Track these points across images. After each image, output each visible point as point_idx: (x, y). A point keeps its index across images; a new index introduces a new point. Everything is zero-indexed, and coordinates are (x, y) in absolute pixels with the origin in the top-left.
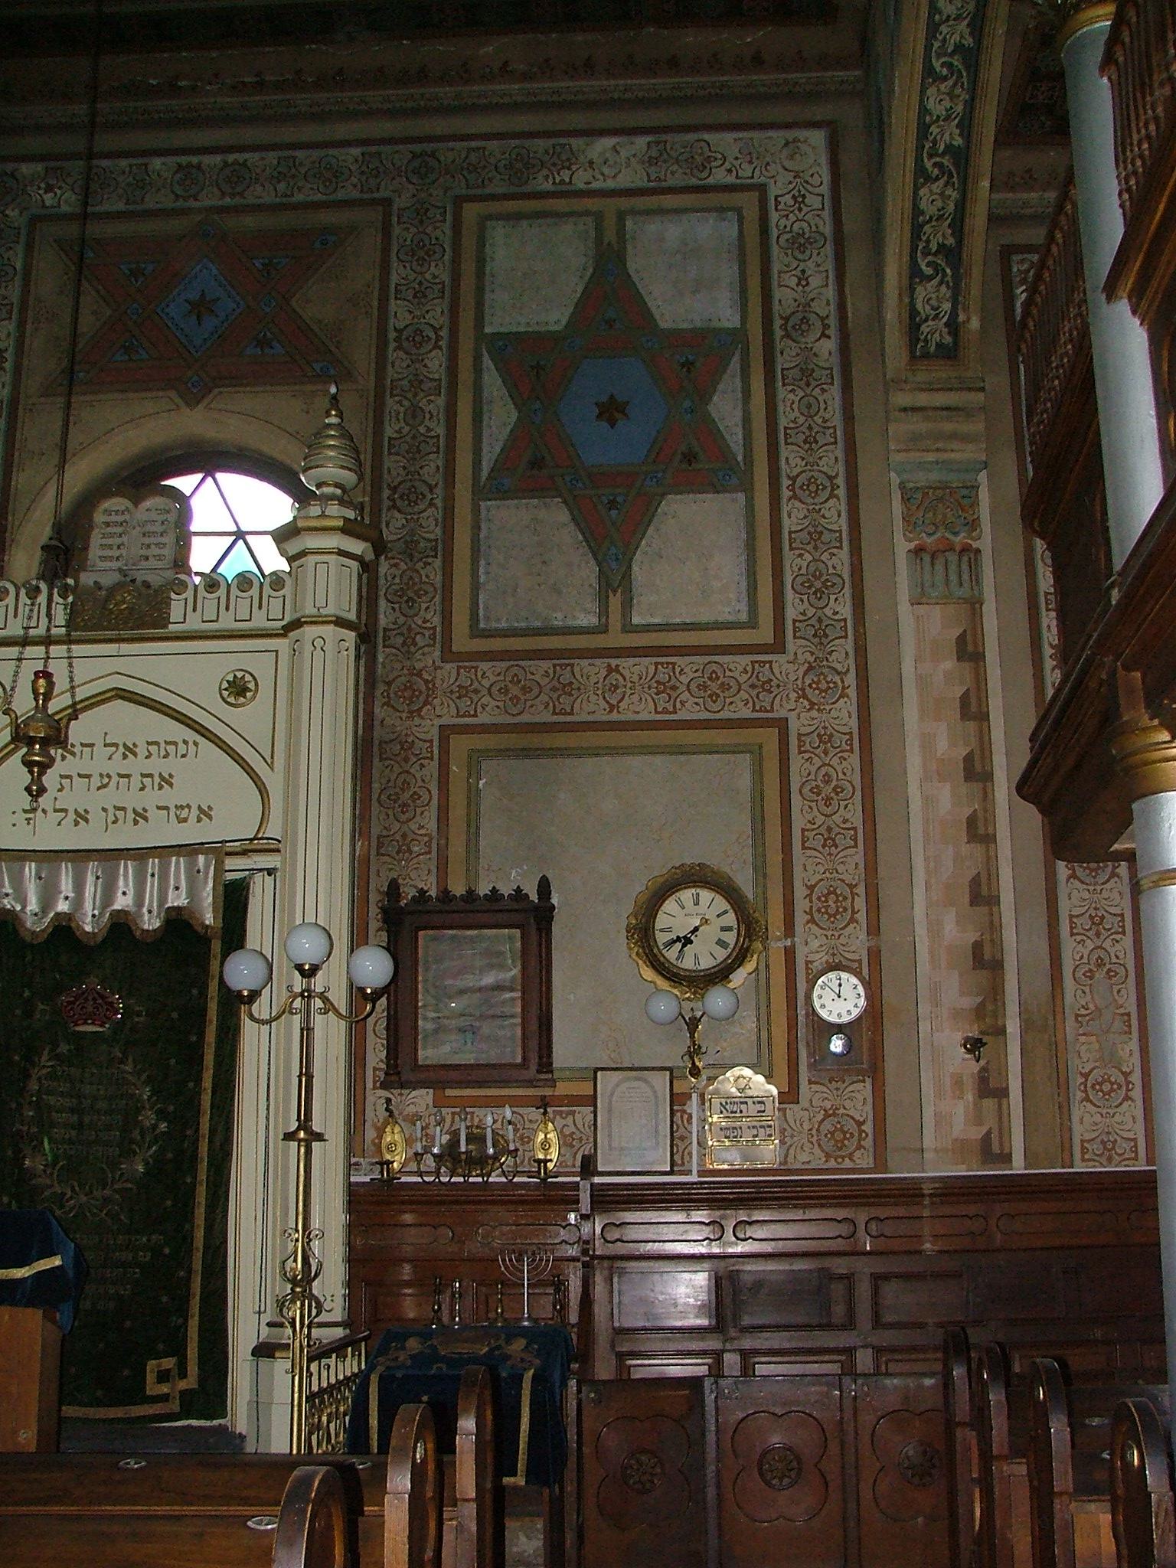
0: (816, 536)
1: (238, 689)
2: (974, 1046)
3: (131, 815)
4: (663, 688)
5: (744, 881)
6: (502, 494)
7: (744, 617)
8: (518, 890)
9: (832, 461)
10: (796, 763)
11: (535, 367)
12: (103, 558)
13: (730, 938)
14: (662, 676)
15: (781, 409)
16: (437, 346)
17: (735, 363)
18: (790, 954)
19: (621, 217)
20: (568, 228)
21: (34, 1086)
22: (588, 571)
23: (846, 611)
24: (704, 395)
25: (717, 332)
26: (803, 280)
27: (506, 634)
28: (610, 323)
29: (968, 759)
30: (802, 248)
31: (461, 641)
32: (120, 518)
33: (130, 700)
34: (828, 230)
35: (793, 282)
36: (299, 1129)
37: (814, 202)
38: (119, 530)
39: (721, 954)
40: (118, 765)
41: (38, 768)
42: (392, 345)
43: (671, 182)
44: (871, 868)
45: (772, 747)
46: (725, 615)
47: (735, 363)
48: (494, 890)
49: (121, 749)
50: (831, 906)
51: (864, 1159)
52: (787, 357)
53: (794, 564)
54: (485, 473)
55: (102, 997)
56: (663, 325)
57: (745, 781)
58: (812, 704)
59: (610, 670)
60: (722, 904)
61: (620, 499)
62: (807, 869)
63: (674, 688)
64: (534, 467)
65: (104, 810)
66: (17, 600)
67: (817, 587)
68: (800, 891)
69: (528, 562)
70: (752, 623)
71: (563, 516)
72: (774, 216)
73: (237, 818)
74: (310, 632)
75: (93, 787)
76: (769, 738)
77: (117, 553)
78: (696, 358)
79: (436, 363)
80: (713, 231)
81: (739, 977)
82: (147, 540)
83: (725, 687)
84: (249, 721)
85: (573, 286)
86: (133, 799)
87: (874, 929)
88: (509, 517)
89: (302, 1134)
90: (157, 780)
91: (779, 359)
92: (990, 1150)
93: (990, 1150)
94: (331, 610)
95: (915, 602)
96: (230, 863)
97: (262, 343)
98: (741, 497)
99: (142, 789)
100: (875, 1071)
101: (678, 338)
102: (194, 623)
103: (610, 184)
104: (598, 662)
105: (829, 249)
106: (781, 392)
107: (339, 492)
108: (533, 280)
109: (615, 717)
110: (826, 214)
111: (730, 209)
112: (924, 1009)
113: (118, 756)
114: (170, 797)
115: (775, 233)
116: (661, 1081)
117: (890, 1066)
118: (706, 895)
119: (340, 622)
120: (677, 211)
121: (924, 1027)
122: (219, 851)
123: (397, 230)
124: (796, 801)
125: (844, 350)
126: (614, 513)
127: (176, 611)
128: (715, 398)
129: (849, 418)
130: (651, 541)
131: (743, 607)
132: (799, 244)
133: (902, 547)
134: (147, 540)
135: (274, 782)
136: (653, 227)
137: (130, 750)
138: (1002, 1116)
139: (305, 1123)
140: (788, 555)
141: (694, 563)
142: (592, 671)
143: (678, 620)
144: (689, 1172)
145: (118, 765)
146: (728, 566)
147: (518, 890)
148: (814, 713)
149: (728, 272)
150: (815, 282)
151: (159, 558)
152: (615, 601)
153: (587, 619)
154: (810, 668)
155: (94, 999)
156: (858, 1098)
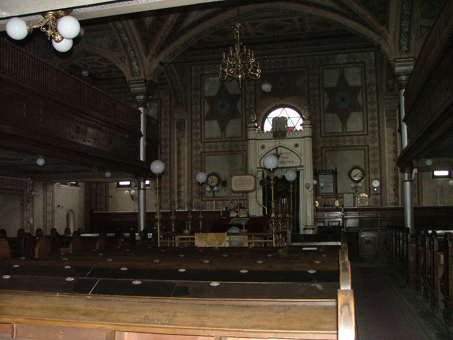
0: (373, 118)
1: (296, 145)
2: (394, 190)
5: (363, 167)
9: (375, 106)
10: (370, 151)
11: (331, 92)
13: (361, 176)
14: (351, 139)
18: (369, 177)
22: (341, 124)
23: (377, 129)
26: (371, 78)
29: (394, 150)
31: (323, 135)
34: (375, 69)
39: (360, 178)
44: (380, 166)
45: (367, 149)
50: (375, 171)
51: (379, 205)
52: (369, 90)
53: (370, 122)
57: (363, 153)
60: (360, 171)
62: (372, 166)
64: (332, 109)
67: (373, 125)
68: (371, 169)
69: (332, 123)
70: (364, 131)
73: (297, 163)
74: (306, 138)
76: (366, 148)
78: (355, 91)
81: (362, 181)
84: (298, 150)
87: (381, 174)
88: (329, 116)
92: (396, 204)
93: (396, 204)
95: (387, 127)
96: (298, 169)
100: (381, 194)
102: (290, 137)
103: (342, 62)
106: (368, 96)
108: (331, 79)
112: (387, 185)
114: (289, 160)
116: (352, 195)
117: (383, 192)
118: (358, 170)
119: (310, 137)
121: (388, 187)
122: (296, 167)
125: (377, 89)
127: (287, 135)
129: (377, 99)
133: (385, 119)
138: (398, 199)
141: (355, 123)
146: (360, 123)
149: (360, 76)
152: (344, 128)
156: (378, 197)
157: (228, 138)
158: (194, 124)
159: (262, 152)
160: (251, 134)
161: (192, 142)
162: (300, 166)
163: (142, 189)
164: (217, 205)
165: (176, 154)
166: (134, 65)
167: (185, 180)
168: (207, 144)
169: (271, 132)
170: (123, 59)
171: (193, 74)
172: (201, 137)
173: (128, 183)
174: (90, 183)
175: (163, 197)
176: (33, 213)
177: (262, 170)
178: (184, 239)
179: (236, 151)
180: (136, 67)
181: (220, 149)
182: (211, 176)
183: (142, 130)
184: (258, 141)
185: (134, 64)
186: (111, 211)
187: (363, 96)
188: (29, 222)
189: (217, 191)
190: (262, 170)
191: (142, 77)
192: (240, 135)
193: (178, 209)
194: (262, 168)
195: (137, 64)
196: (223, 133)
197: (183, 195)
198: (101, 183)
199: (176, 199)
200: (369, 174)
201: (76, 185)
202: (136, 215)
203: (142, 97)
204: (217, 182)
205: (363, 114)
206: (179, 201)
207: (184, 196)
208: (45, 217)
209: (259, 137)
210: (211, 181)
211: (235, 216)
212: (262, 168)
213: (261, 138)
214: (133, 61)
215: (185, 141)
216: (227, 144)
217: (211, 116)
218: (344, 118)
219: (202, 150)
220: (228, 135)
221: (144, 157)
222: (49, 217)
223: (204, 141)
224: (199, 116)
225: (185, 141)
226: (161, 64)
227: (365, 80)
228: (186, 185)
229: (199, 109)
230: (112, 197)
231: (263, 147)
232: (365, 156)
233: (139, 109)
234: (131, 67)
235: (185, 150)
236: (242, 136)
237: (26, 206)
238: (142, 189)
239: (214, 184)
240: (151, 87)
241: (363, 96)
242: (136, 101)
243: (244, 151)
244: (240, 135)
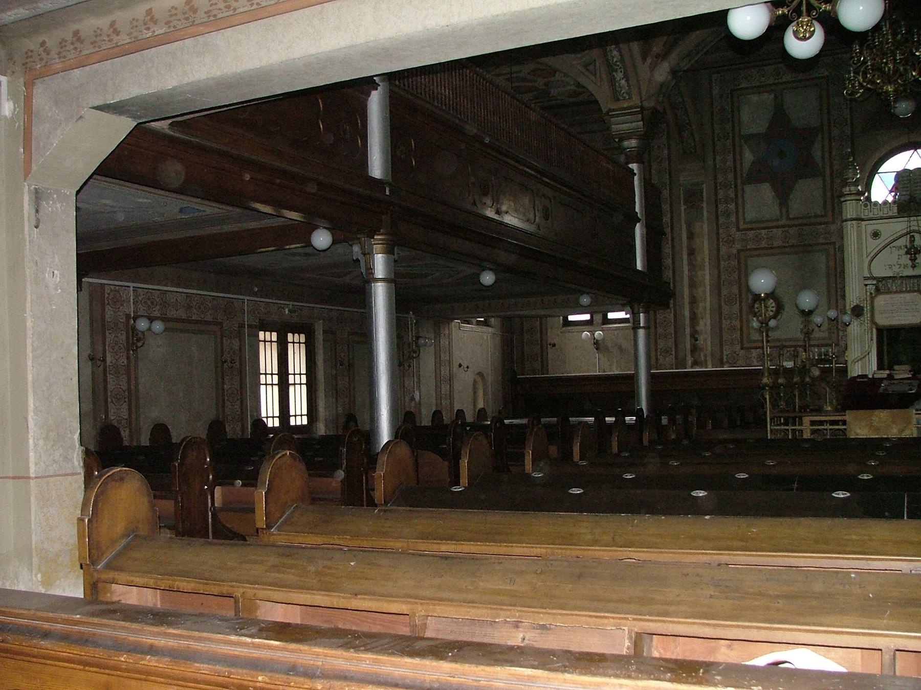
41: (913, 260)
158: (721, 193)
160: (850, 209)
161: (718, 229)
163: (643, 327)
165: (685, 257)
166: (618, 79)
167: (705, 308)
168: (751, 234)
169: (894, 202)
170: (591, 68)
171: (716, 91)
172: (737, 219)
173: (587, 317)
174: (509, 318)
175: (661, 344)
176: (419, 382)
177: (875, 282)
178: (821, 423)
179: (815, 246)
180: (623, 82)
181: (777, 243)
183: (637, 210)
184: (864, 223)
185: (619, 75)
186: (555, 372)
188: (413, 399)
189: (776, 328)
190: (875, 282)
191: (636, 101)
193: (692, 367)
194: (874, 278)
195: (626, 76)
196: (784, 210)
197: (701, 338)
198: (532, 317)
199: (688, 346)
201: (486, 323)
202: (630, 380)
203: (633, 143)
206: (694, 349)
207: (705, 340)
208: (438, 387)
209: (866, 214)
211: (885, 376)
213: (871, 215)
214: (616, 71)
215: (704, 228)
216: (792, 231)
217: (757, 175)
219: (738, 246)
221: (643, 262)
222: (445, 388)
223: (746, 226)
224: (731, 176)
225: (704, 228)
226: (674, 72)
228: (708, 316)
229: (730, 164)
230: (554, 345)
231: (876, 235)
233: (630, 166)
234: (612, 81)
235: (705, 245)
237: (409, 366)
238: (643, 327)
240: (653, 121)
242: (622, 150)
243: (830, 243)
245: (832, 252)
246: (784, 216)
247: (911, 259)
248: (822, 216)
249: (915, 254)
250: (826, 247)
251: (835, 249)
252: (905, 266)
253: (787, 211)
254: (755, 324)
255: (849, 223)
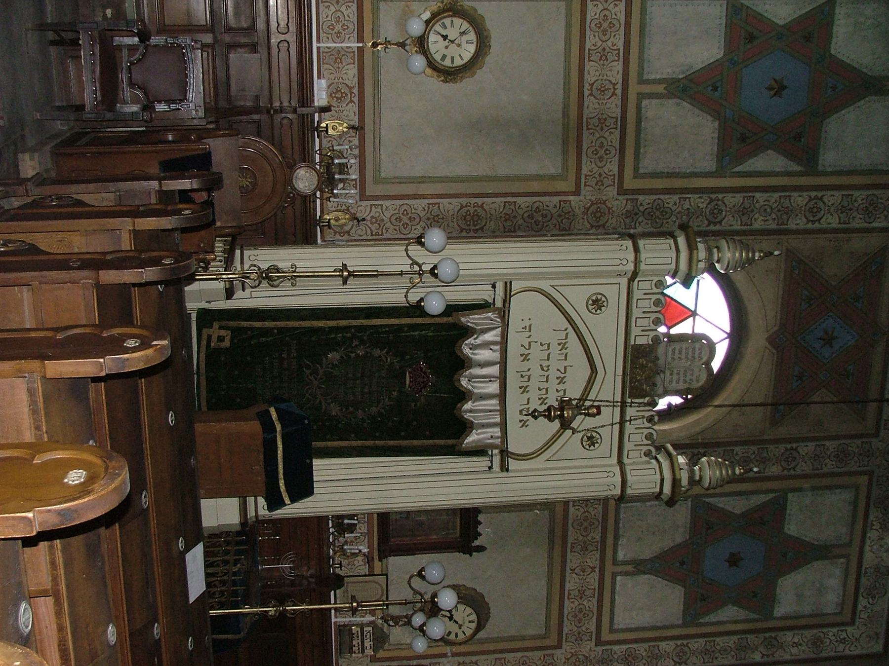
3: (525, 384)
4: (582, 594)
6: (694, 510)
7: (615, 627)
8: (480, 535)
11: (767, 519)
12: (674, 351)
15: (726, 638)
16: (784, 469)
17: (752, 616)
19: (847, 556)
20: (844, 530)
21: (377, 352)
22: (647, 554)
24: (737, 603)
25: (773, 608)
26: (796, 645)
27: (617, 522)
28: (785, 555)
30: (814, 643)
32: (696, 355)
33: (589, 382)
34: (824, 654)
35: (796, 640)
36: (349, 271)
37: (841, 647)
38: (690, 356)
40: (553, 374)
42: (789, 446)
43: (863, 580)
45: (547, 642)
46: (617, 619)
47: (752, 616)
48: (480, 523)
49: (562, 376)
54: (707, 500)
55: (425, 387)
56: (779, 581)
57: (531, 632)
58: (568, 659)
59: (593, 569)
61: (685, 566)
63: (585, 542)
65: (529, 370)
66: (652, 312)
68: (474, 659)
71: (679, 540)
72: (835, 630)
75: (541, 362)
77: (676, 357)
78: (759, 597)
79: (774, 470)
80: (831, 601)
82: (682, 373)
83: (580, 621)
85: (810, 535)
86: (534, 384)
89: (346, 274)
90: (544, 397)
91: (752, 636)
94: (629, 491)
97: (800, 378)
98: (680, 622)
99: (540, 389)
101: (773, 585)
104: (598, 562)
105: (812, 656)
106: (735, 638)
107: (697, 478)
109: (568, 571)
110: (833, 654)
111: (842, 608)
113: (559, 374)
115: (825, 630)
120: (845, 585)
123: (859, 442)
124: (520, 654)
126: (678, 564)
128: (735, 608)
130: (659, 583)
131: (621, 626)
132: (816, 643)
134: (682, 373)
135: (538, 463)
136: (838, 572)
137: (561, 381)
139: (351, 274)
140: (646, 645)
142: (593, 559)
143: (617, 597)
144: (336, 617)
145: (553, 374)
146: (643, 618)
147: (480, 535)
148: (563, 660)
149: (807, 609)
150: (794, 651)
151: (671, 382)
152: (629, 568)
153: (621, 555)
154: (587, 658)
155: (424, 382)
157: (639, 108)
159: (577, 297)
160: (657, 252)
162: (505, 454)
164: (338, 56)
177: (499, 304)
182: (472, 36)
184: (624, 281)
187: (736, 622)
189: (405, 64)
190: (499, 304)
192: (648, 164)
194: (506, 300)
196: (660, 88)
200: (454, 655)
204: (447, 63)
205: (672, 627)
210: (453, 34)
212: (506, 300)
213: (637, 294)
216: (613, 107)
218: (663, 565)
220: (651, 108)
227: (790, 628)
232: (523, 638)
236: (645, 176)
239: (435, 44)
241: (736, 622)
244: (648, 164)
245: (562, 186)
246: (646, 89)
247: (549, 409)
248: (636, 169)
249: (561, 417)
250: (572, 177)
251: (565, 193)
252: (543, 401)
253: (658, 96)
254: (416, 27)
255: (631, 256)
